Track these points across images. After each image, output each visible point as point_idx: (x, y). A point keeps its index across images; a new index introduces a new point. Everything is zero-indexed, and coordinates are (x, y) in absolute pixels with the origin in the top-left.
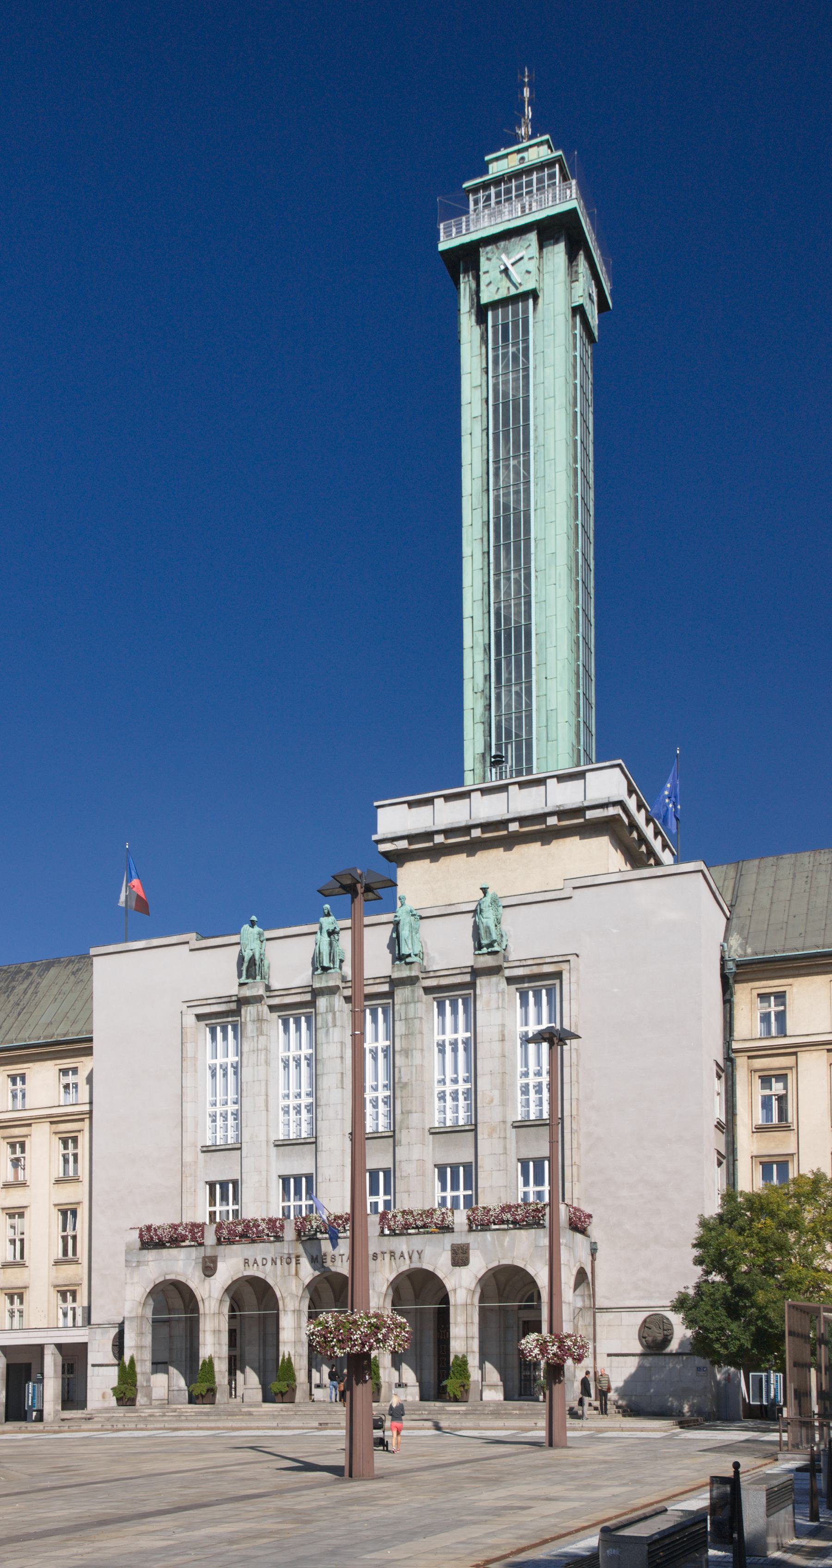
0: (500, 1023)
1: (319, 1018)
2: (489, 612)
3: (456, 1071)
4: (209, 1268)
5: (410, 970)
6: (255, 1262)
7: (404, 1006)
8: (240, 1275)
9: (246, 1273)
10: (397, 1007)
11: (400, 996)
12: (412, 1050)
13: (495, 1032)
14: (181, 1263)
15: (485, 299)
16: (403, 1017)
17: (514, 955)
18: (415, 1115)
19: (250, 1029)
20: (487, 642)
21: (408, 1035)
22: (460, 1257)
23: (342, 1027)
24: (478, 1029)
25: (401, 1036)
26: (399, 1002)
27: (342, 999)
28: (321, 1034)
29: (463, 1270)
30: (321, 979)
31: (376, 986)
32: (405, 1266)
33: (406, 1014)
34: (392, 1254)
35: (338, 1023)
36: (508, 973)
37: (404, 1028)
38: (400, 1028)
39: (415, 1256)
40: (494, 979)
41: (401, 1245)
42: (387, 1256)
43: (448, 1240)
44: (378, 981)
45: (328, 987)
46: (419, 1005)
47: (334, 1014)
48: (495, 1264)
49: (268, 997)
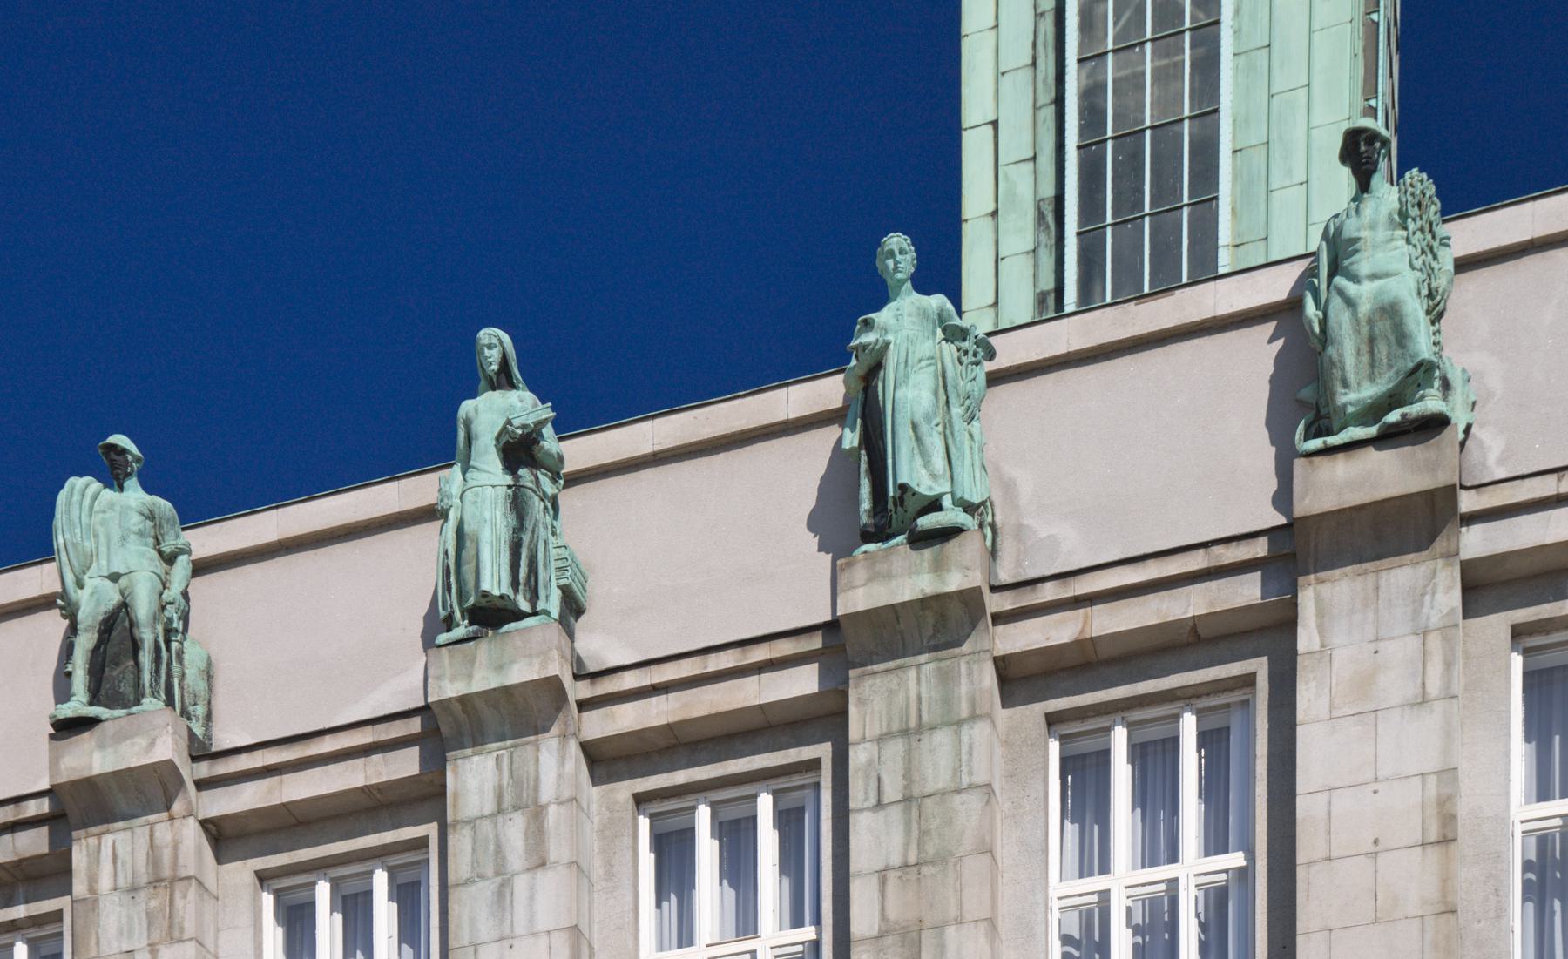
0: (1432, 763)
2: (1059, 101)
5: (938, 567)
7: (896, 748)
11: (878, 704)
12: (940, 928)
13: (1404, 809)
16: (892, 792)
20: (1048, 190)
23: (575, 864)
25: (883, 875)
26: (874, 730)
27: (573, 748)
30: (471, 661)
31: (751, 682)
33: (908, 775)
37: (896, 839)
44: (760, 654)
45: (507, 691)
46: (978, 733)
49: (202, 785)
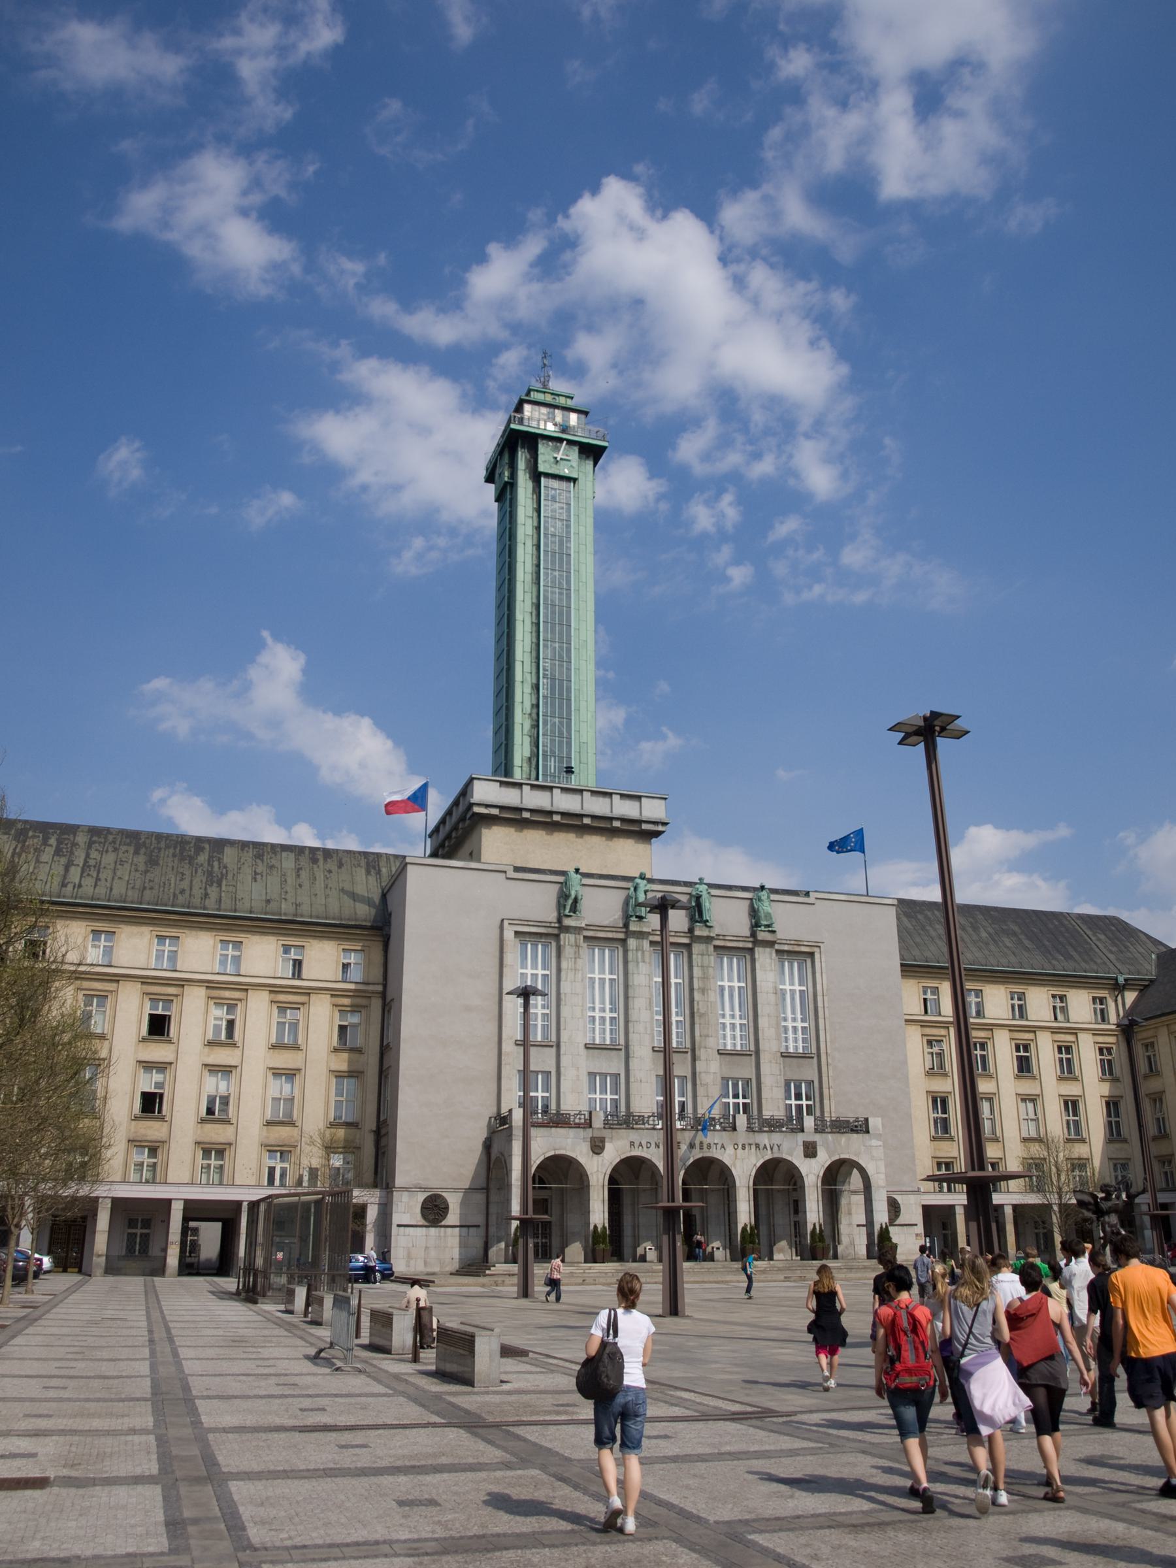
1: (630, 954)
3: (732, 1009)
4: (597, 1147)
6: (641, 1145)
8: (628, 1155)
9: (634, 1153)
10: (694, 957)
14: (569, 1141)
15: (541, 468)
17: (779, 935)
18: (711, 1039)
19: (568, 951)
21: (705, 978)
22: (810, 1151)
24: (758, 983)
28: (631, 966)
29: (813, 1161)
32: (768, 1156)
34: (757, 1146)
35: (647, 960)
36: (777, 947)
38: (697, 972)
39: (776, 1148)
40: (768, 950)
41: (764, 1139)
42: (753, 1147)
43: (801, 1138)
47: (643, 952)
48: (837, 1157)
